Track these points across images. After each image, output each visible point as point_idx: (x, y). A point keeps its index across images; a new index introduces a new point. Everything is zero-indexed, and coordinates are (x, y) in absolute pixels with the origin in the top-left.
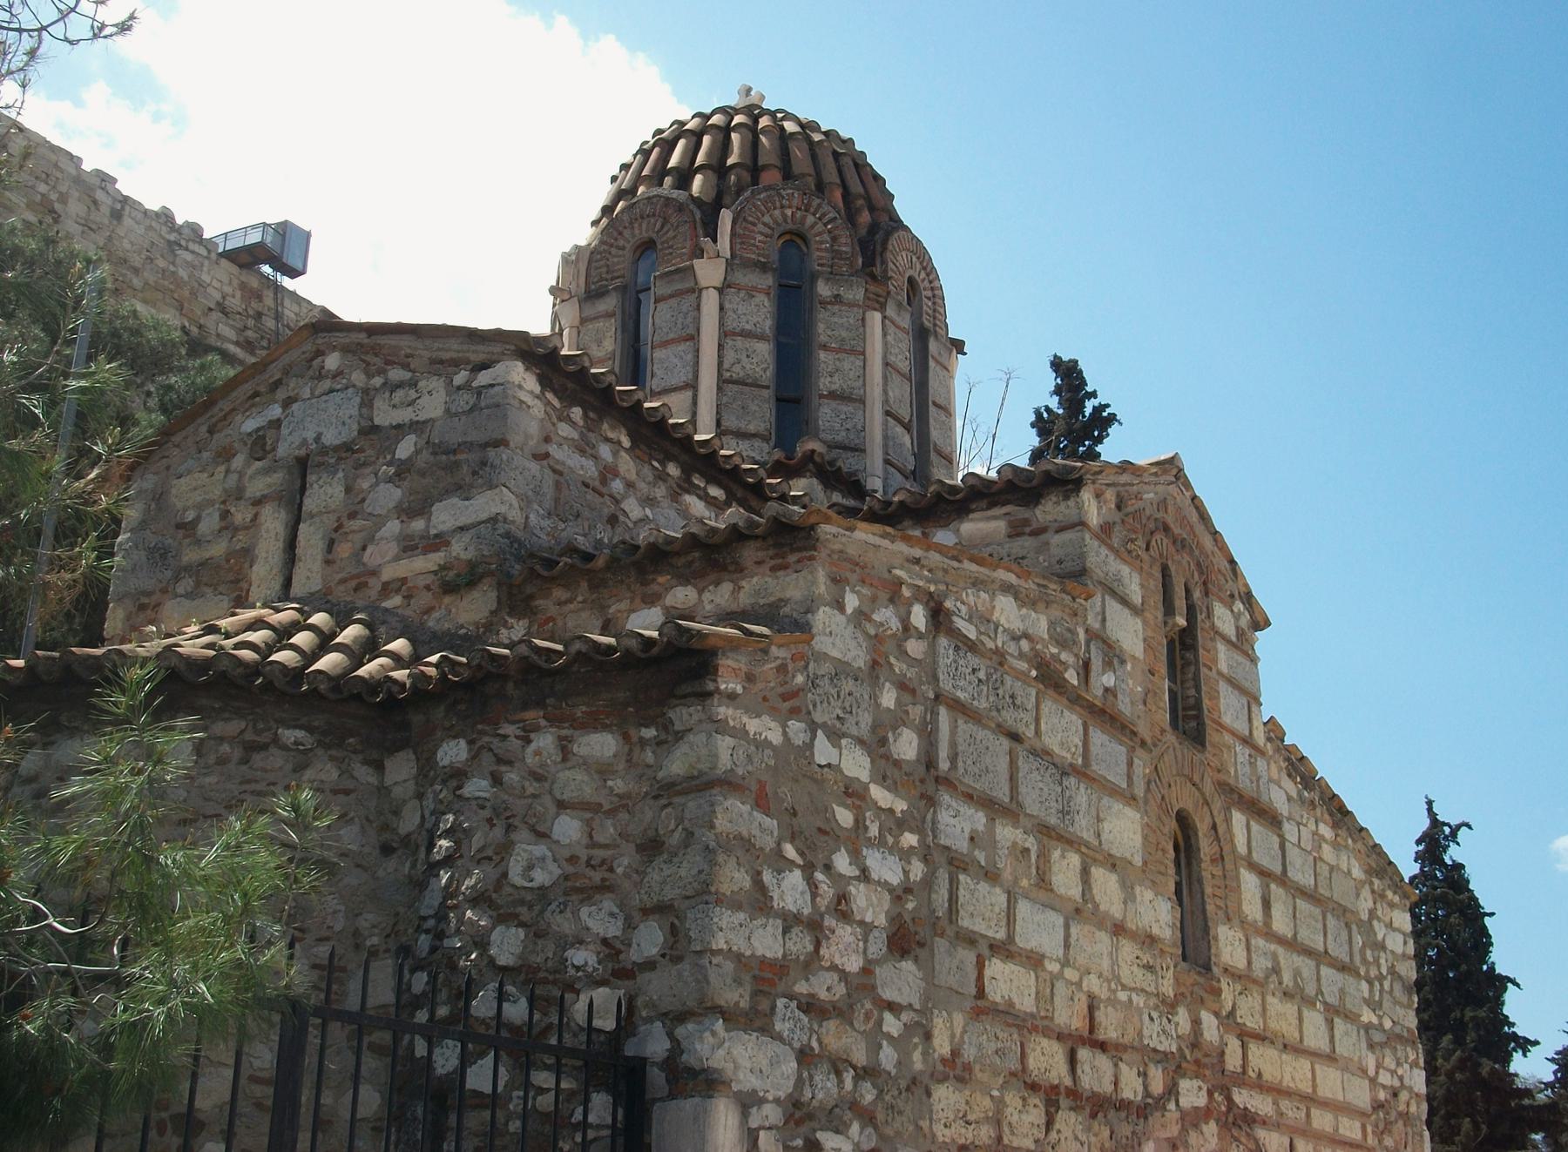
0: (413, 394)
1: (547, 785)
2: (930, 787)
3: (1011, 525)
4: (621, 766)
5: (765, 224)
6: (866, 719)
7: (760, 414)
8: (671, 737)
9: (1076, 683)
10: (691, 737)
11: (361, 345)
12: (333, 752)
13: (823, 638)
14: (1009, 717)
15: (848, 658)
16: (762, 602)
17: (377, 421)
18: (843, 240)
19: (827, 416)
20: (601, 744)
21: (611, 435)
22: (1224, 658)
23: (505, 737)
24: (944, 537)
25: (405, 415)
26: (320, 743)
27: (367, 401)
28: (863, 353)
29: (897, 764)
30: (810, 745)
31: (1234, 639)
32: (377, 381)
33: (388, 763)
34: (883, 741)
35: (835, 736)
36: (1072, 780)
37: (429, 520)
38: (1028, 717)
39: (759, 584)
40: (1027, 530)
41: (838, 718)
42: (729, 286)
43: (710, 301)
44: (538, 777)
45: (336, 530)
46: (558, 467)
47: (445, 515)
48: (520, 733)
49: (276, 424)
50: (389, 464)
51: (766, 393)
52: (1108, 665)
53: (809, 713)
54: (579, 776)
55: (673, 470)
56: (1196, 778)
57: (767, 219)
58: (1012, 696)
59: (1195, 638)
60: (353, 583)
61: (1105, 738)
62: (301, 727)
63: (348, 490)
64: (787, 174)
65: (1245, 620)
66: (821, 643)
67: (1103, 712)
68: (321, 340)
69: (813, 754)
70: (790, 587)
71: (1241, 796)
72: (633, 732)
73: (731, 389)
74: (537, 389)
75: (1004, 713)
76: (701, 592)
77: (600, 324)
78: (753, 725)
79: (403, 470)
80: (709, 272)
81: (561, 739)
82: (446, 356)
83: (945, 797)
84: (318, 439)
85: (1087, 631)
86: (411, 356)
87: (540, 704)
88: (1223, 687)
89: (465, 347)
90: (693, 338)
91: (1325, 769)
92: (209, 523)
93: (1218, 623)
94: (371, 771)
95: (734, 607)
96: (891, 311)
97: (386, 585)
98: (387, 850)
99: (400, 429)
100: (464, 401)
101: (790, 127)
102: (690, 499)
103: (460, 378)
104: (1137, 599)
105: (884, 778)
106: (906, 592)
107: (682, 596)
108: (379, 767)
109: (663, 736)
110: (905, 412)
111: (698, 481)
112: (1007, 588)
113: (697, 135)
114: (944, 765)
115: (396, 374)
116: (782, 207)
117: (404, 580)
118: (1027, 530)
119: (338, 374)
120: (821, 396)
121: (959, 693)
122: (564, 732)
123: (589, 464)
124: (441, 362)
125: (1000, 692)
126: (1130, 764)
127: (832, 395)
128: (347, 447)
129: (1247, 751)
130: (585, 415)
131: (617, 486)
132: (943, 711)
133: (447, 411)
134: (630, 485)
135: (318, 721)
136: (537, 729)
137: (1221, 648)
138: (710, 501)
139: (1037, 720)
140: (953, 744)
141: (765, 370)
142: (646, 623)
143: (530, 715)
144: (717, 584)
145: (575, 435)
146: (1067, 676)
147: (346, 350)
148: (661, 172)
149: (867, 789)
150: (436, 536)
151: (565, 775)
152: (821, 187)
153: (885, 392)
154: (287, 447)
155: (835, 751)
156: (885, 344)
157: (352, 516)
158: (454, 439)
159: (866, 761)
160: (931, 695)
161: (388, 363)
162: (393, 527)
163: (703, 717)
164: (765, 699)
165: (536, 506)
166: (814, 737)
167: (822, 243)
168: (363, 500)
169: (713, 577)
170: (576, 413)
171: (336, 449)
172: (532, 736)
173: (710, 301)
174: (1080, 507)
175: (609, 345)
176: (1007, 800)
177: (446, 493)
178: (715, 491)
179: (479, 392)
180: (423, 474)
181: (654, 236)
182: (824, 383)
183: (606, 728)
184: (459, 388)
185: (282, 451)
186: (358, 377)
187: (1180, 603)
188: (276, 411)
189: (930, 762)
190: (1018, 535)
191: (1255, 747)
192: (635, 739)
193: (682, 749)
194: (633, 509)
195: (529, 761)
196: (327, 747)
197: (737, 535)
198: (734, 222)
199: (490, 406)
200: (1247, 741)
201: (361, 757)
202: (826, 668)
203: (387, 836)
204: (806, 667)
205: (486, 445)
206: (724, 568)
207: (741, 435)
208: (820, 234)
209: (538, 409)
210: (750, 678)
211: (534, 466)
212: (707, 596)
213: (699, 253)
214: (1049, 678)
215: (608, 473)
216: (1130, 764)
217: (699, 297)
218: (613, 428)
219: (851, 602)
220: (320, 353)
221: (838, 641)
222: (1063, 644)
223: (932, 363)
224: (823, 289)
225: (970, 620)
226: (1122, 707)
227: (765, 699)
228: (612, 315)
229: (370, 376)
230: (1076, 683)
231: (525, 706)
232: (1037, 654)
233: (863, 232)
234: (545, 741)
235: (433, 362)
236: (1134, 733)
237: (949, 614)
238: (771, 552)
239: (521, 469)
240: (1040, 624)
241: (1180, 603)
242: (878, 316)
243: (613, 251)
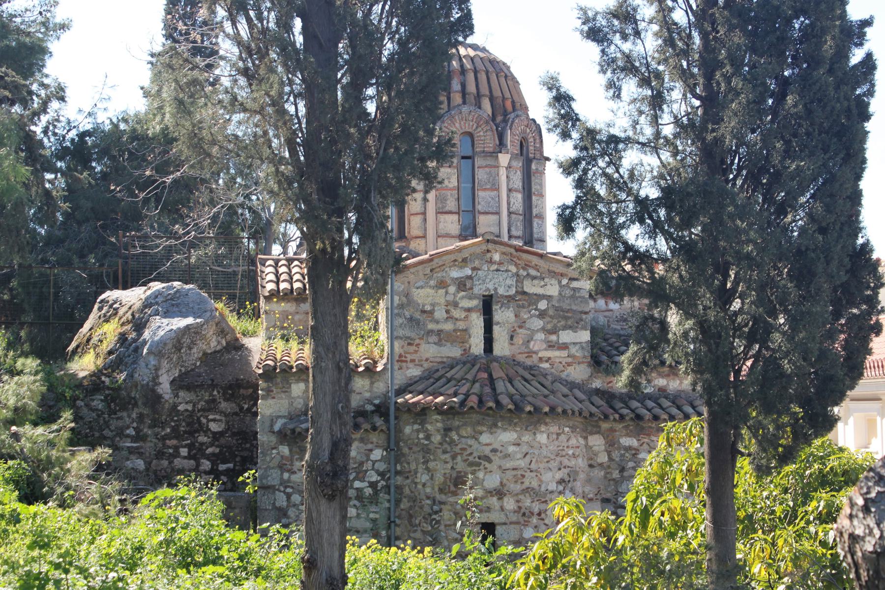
11: (511, 254)
17: (525, 289)
25: (541, 291)
27: (519, 279)
37: (558, 336)
43: (503, 173)
49: (470, 278)
50: (536, 309)
68: (490, 246)
73: (513, 216)
79: (542, 314)
90: (498, 189)
92: (440, 314)
95: (680, 388)
97: (541, 359)
98: (591, 466)
100: (568, 293)
103: (565, 281)
108: (586, 438)
115: (533, 272)
119: (500, 263)
133: (560, 294)
154: (479, 289)
162: (541, 336)
173: (503, 173)
177: (565, 328)
179: (574, 289)
185: (476, 290)
188: (468, 272)
203: (590, 462)
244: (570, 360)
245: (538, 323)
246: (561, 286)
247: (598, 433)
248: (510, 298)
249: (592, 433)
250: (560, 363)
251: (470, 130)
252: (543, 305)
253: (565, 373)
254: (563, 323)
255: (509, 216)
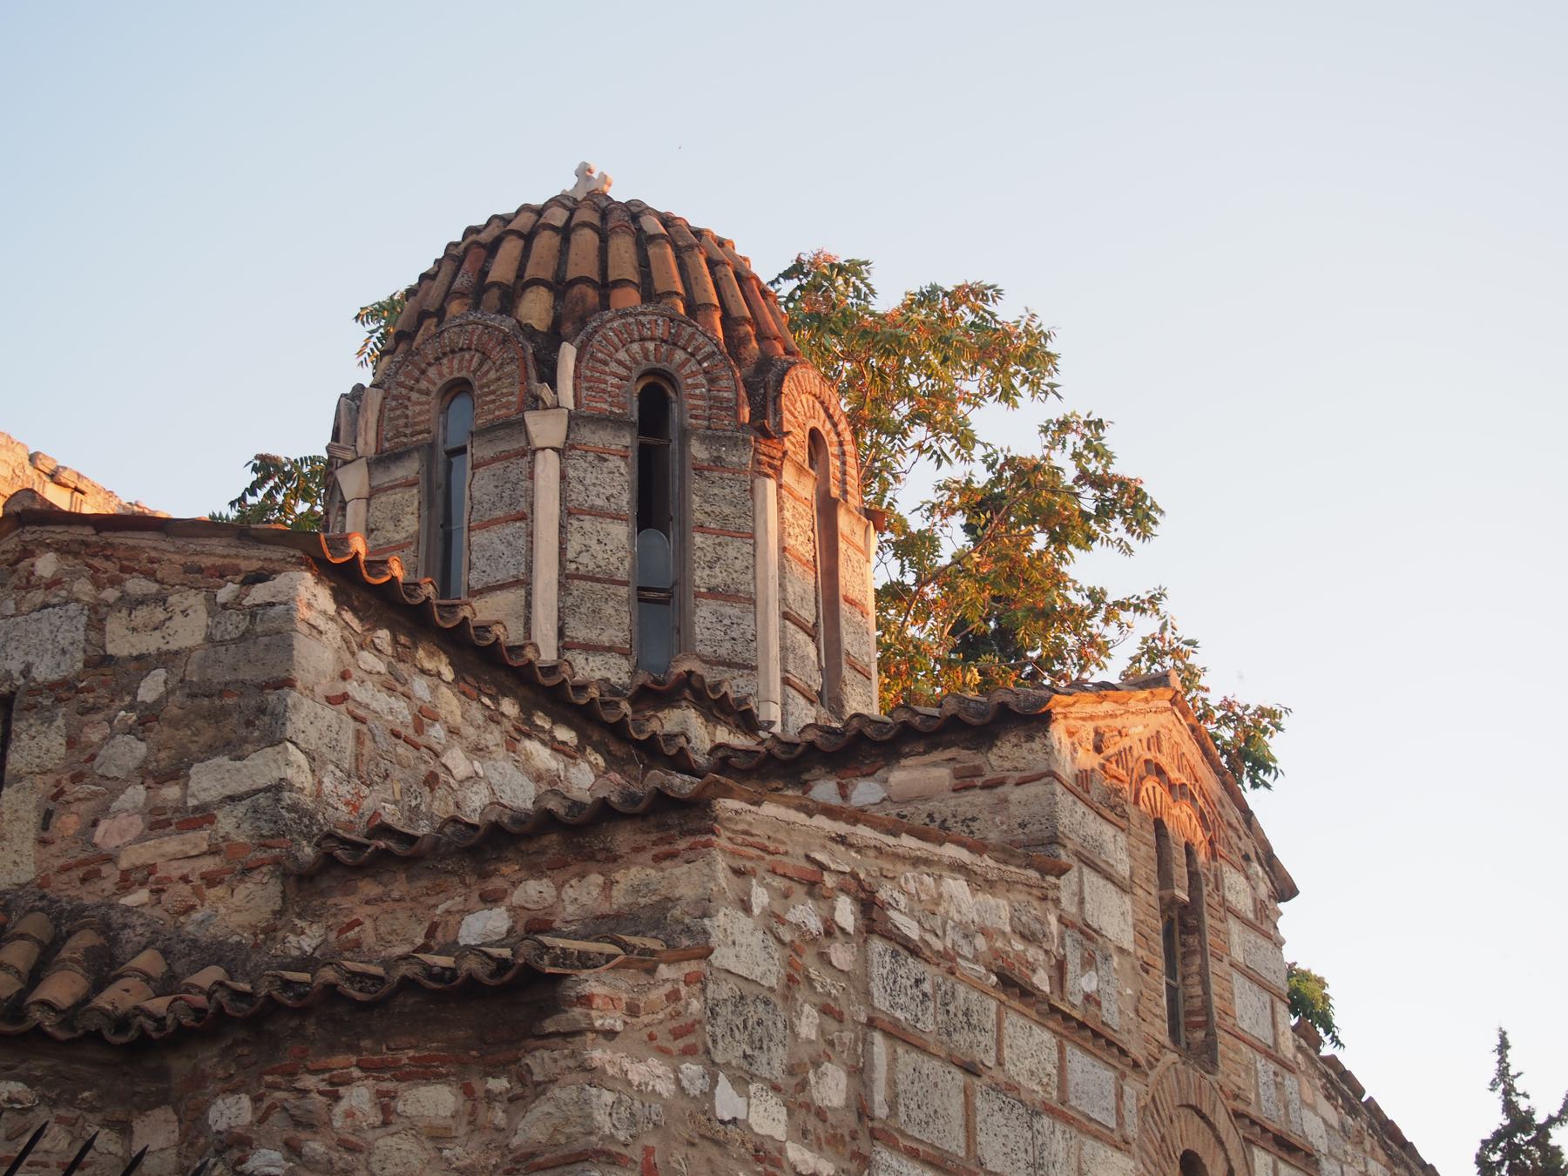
0: (160, 615)
1: (361, 1157)
2: (864, 1144)
3: (958, 775)
4: (463, 1130)
5: (620, 363)
6: (779, 1056)
7: (614, 620)
8: (528, 1091)
9: (1047, 989)
10: (556, 1091)
11: (83, 543)
12: (62, 1112)
13: (724, 950)
14: (962, 1039)
15: (756, 974)
16: (642, 901)
17: (109, 652)
18: (724, 383)
19: (704, 618)
20: (435, 1101)
21: (428, 665)
22: (1239, 941)
23: (304, 1092)
24: (865, 792)
25: (151, 643)
26: (42, 1097)
27: (96, 623)
28: (752, 536)
29: (821, 1114)
30: (709, 1095)
31: (1251, 916)
32: (111, 594)
33: (138, 1126)
34: (803, 1085)
35: (741, 1082)
36: (1046, 1121)
37: (186, 786)
38: (987, 1040)
39: (635, 879)
40: (979, 781)
41: (745, 1056)
42: (573, 447)
44: (352, 1148)
45: (55, 798)
46: (360, 712)
47: (209, 780)
48: (324, 1087)
50: (130, 708)
51: (623, 591)
52: (1088, 962)
53: (708, 1052)
54: (407, 1144)
55: (509, 707)
56: (1206, 1110)
57: (622, 355)
58: (966, 1013)
59: (1200, 918)
60: (80, 872)
61: (1087, 1060)
62: (16, 1078)
63: (71, 743)
64: (649, 294)
65: (1264, 889)
66: (723, 957)
67: (1082, 1026)
68: (30, 534)
69: (713, 1107)
70: (682, 881)
71: (1264, 1130)
72: (477, 1084)
73: (578, 586)
74: (331, 608)
75: (956, 1037)
76: (559, 888)
77: (397, 496)
78: (637, 1072)
79: (148, 718)
80: (546, 429)
81: (380, 1094)
82: (206, 562)
83: (884, 1156)
84: (26, 672)
85: (1060, 920)
86: (159, 561)
87: (351, 1048)
88: (1239, 981)
89: (233, 551)
90: (525, 517)
91: (1374, 1087)
93: (1230, 896)
94: (113, 1136)
95: (605, 908)
96: (788, 475)
97: (125, 874)
99: (144, 663)
100: (234, 624)
101: (653, 226)
102: (532, 746)
103: (226, 593)
104: (1123, 868)
105: (805, 1133)
106: (829, 881)
107: (534, 891)
108: (124, 1129)
109: (518, 1090)
110: (808, 614)
111: (541, 720)
112: (959, 868)
113: (528, 238)
114: (881, 1111)
116: (643, 339)
117: (151, 869)
118: (979, 781)
119: (55, 582)
120: (698, 595)
121: (899, 1014)
122: (386, 1086)
123: (400, 705)
124: (200, 570)
125: (951, 1008)
126: (1120, 1095)
127: (713, 593)
128: (66, 684)
129: (1272, 1067)
130: (395, 641)
131: (437, 732)
132: (878, 1037)
133: (209, 638)
134: (453, 731)
135: (39, 1066)
136: (348, 1082)
137: (1234, 926)
138: (557, 747)
139: (999, 1042)
140: (892, 1083)
141: (622, 561)
142: (484, 926)
143: (339, 1060)
144: (582, 876)
145: (382, 668)
146: (1035, 980)
147: (62, 549)
148: (481, 287)
149: (782, 1150)
150: (196, 809)
151: (385, 1143)
152: (693, 308)
153: (782, 586)
155: (741, 1102)
156: (782, 521)
157: (77, 778)
158: (220, 676)
159: (782, 1114)
160: (863, 1019)
161: (123, 569)
162: (136, 795)
163: (571, 1063)
164: (652, 1037)
165: (331, 767)
166: (714, 1083)
167: (696, 386)
168: (93, 757)
169: (576, 868)
170: (383, 636)
171: (52, 686)
172: (342, 1090)
173: (547, 468)
174: (1049, 751)
175: (410, 524)
176: (962, 1154)
177: (211, 751)
178: (565, 735)
179: (253, 612)
180: (174, 724)
181: (470, 377)
182: (701, 577)
183: (440, 1078)
184: (224, 606)
186: (83, 588)
187: (1180, 872)
189: (863, 1111)
190: (967, 788)
191: (1282, 1063)
192: (480, 1093)
193: (541, 1108)
194: (458, 762)
195: (337, 1124)
196: (54, 1104)
197: (603, 813)
198: (578, 360)
199: (271, 634)
200: (1271, 1053)
201: (99, 1117)
202: (723, 990)
204: (704, 990)
205: (267, 685)
206: (592, 857)
207: (590, 648)
208: (693, 374)
209: (332, 631)
210: (633, 1010)
211: (329, 714)
212: (569, 893)
213: (536, 403)
214: (1012, 984)
215: (425, 716)
216: (1120, 1095)
217: (532, 463)
218: (431, 655)
219: (760, 898)
220: (27, 553)
221: (743, 954)
222: (1028, 937)
223: (842, 545)
224: (698, 451)
225: (911, 914)
226: (1107, 1018)
227: (652, 1037)
228: (410, 484)
229: (99, 586)
230: (1047, 989)
231: (332, 1049)
232: (997, 954)
233: (748, 370)
234: (359, 1097)
235: (189, 569)
236: (1123, 1052)
237: (884, 906)
238: (653, 837)
239: (309, 718)
240: (998, 910)
241: (1180, 872)
242: (771, 485)
243: (414, 396)
244: (209, 864)
245: (129, 752)
246: (216, 609)
247: (162, 1100)
248: (63, 689)
249: (146, 1105)
250: (185, 879)
251: (464, 374)
252: (151, 688)
253: (196, 916)
254: (208, 734)
255: (562, 586)
